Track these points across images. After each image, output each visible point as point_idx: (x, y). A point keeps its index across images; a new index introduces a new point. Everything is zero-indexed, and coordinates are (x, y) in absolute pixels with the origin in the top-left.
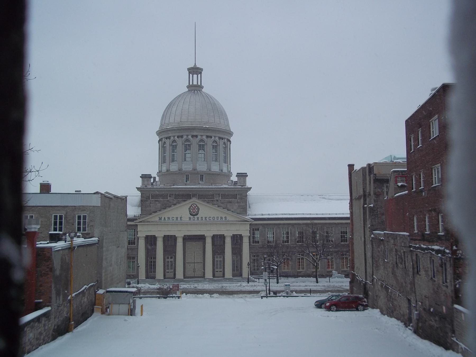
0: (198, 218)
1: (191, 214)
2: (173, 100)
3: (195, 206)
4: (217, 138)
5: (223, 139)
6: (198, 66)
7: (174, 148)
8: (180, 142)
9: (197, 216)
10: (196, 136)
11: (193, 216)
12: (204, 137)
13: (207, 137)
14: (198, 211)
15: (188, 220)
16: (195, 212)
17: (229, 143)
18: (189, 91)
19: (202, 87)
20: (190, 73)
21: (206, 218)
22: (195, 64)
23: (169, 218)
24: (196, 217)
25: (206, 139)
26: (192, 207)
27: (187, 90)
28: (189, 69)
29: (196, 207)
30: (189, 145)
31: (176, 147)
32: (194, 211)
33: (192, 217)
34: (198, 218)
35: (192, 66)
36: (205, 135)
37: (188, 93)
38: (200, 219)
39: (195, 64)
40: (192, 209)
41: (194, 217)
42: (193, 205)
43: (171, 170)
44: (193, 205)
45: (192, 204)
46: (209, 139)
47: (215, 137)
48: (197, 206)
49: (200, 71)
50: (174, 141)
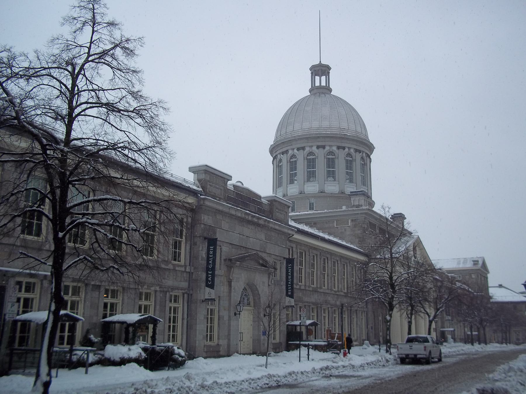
4: (352, 151)
5: (360, 152)
8: (300, 156)
13: (339, 148)
30: (314, 160)
31: (296, 164)
36: (335, 146)
47: (349, 148)
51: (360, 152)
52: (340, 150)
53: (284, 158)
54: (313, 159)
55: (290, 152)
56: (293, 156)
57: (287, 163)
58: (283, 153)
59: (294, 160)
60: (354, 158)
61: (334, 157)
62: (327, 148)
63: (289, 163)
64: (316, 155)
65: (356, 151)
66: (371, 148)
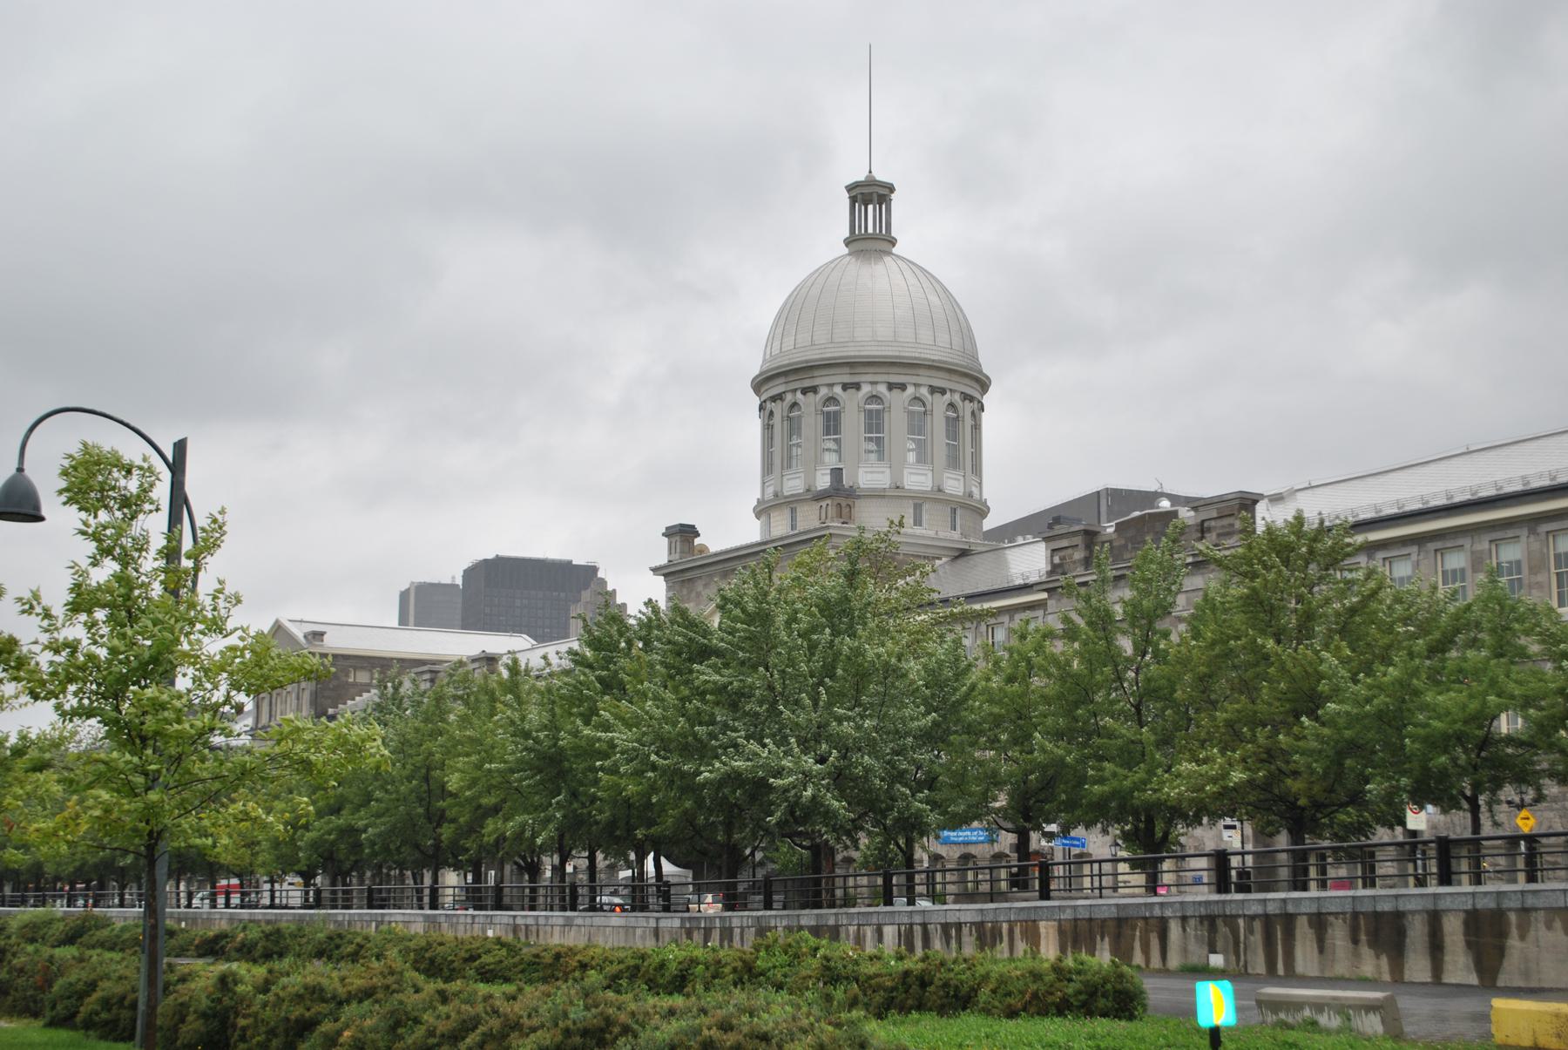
2: (805, 281)
6: (880, 176)
7: (793, 426)
10: (903, 387)
12: (924, 391)
17: (968, 406)
18: (850, 254)
19: (893, 242)
20: (853, 200)
22: (870, 172)
25: (929, 397)
27: (846, 251)
28: (850, 188)
35: (861, 176)
37: (848, 258)
39: (870, 172)
43: (786, 494)
46: (937, 395)
49: (882, 191)
50: (794, 405)
51: (943, 391)
52: (895, 390)
53: (778, 408)
54: (878, 411)
55: (789, 398)
56: (794, 405)
57: (783, 421)
58: (774, 399)
59: (795, 414)
60: (929, 407)
61: (880, 407)
62: (910, 390)
63: (785, 422)
64: (887, 405)
65: (933, 390)
66: (984, 384)
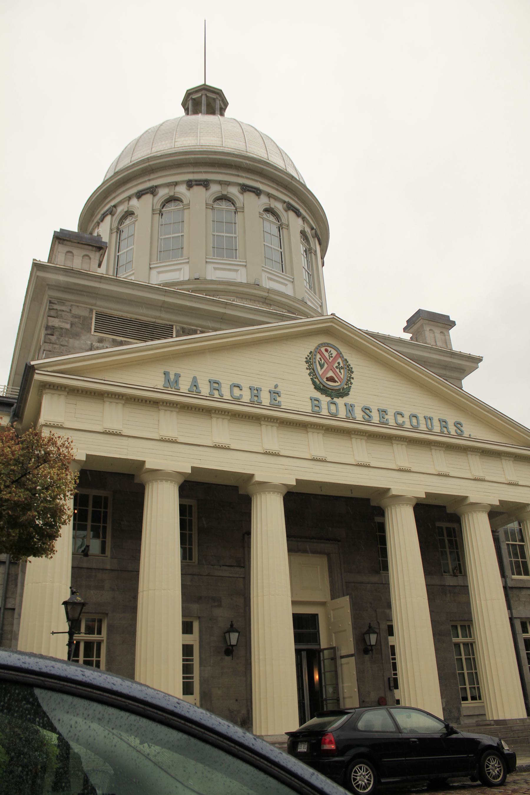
0: (350, 408)
1: (317, 388)
3: (334, 353)
9: (346, 399)
11: (329, 399)
14: (349, 380)
15: (307, 407)
16: (335, 381)
21: (383, 412)
23: (215, 385)
24: (340, 401)
26: (318, 356)
29: (340, 360)
32: (330, 374)
33: (324, 399)
34: (350, 408)
38: (359, 415)
40: (322, 366)
41: (334, 403)
42: (326, 350)
44: (323, 349)
45: (320, 342)
48: (340, 354)
